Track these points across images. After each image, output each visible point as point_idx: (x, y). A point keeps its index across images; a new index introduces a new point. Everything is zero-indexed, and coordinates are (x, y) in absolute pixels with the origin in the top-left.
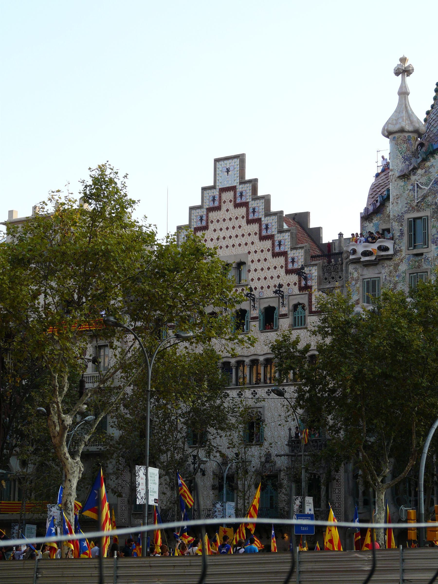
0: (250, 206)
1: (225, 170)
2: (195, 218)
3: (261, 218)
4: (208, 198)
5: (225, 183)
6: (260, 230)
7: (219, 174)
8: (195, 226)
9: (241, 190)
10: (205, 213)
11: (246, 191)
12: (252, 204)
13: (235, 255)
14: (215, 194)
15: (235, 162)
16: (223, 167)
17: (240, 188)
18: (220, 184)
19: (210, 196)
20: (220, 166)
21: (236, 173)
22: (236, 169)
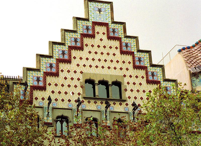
0: (123, 41)
1: (97, 9)
2: (69, 38)
3: (133, 52)
4: (81, 26)
5: (98, 18)
6: (134, 61)
7: (91, 11)
8: (69, 45)
9: (113, 27)
10: (79, 36)
11: (118, 29)
12: (125, 40)
13: (111, 75)
14: (88, 25)
15: (106, 6)
16: (95, 7)
17: (112, 26)
18: (93, 18)
19: (83, 25)
20: (92, 6)
21: (107, 14)
22: (107, 11)
